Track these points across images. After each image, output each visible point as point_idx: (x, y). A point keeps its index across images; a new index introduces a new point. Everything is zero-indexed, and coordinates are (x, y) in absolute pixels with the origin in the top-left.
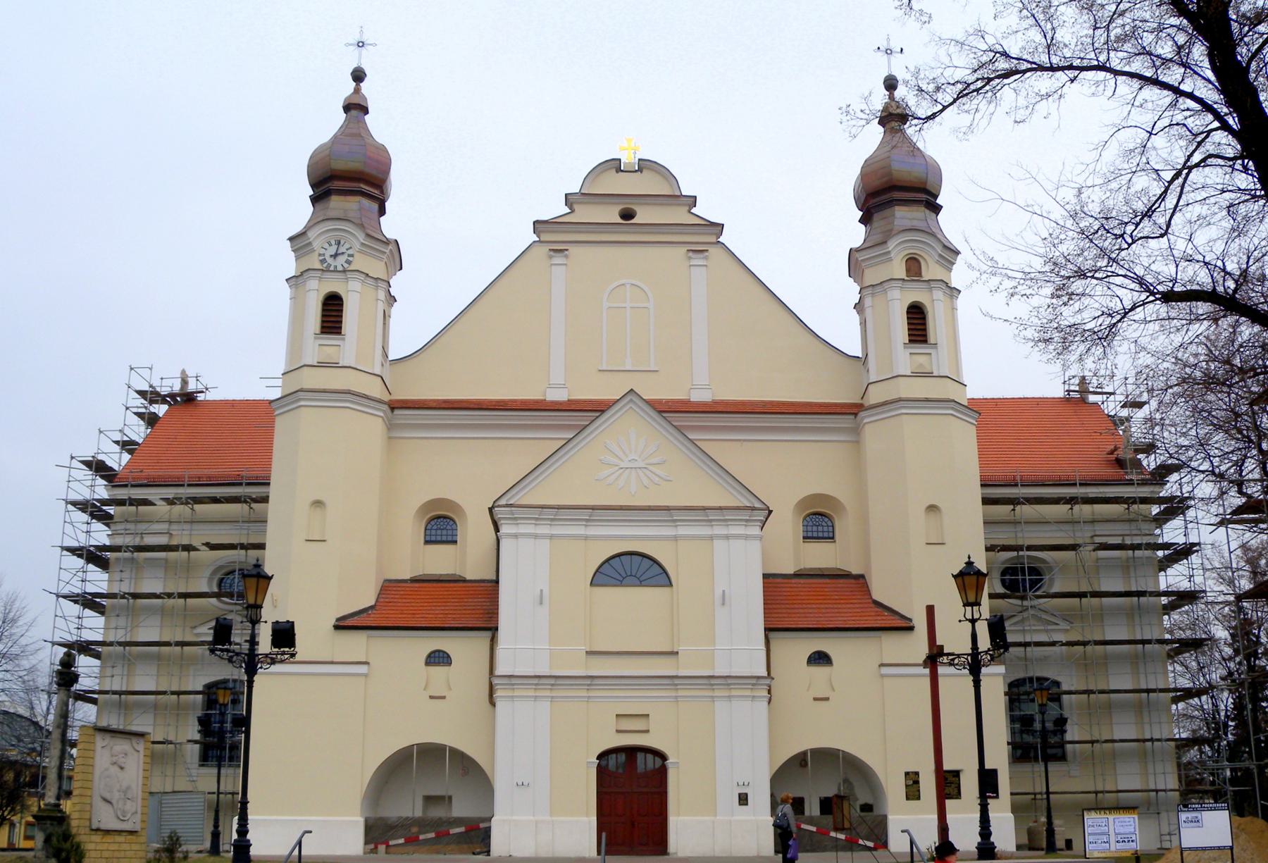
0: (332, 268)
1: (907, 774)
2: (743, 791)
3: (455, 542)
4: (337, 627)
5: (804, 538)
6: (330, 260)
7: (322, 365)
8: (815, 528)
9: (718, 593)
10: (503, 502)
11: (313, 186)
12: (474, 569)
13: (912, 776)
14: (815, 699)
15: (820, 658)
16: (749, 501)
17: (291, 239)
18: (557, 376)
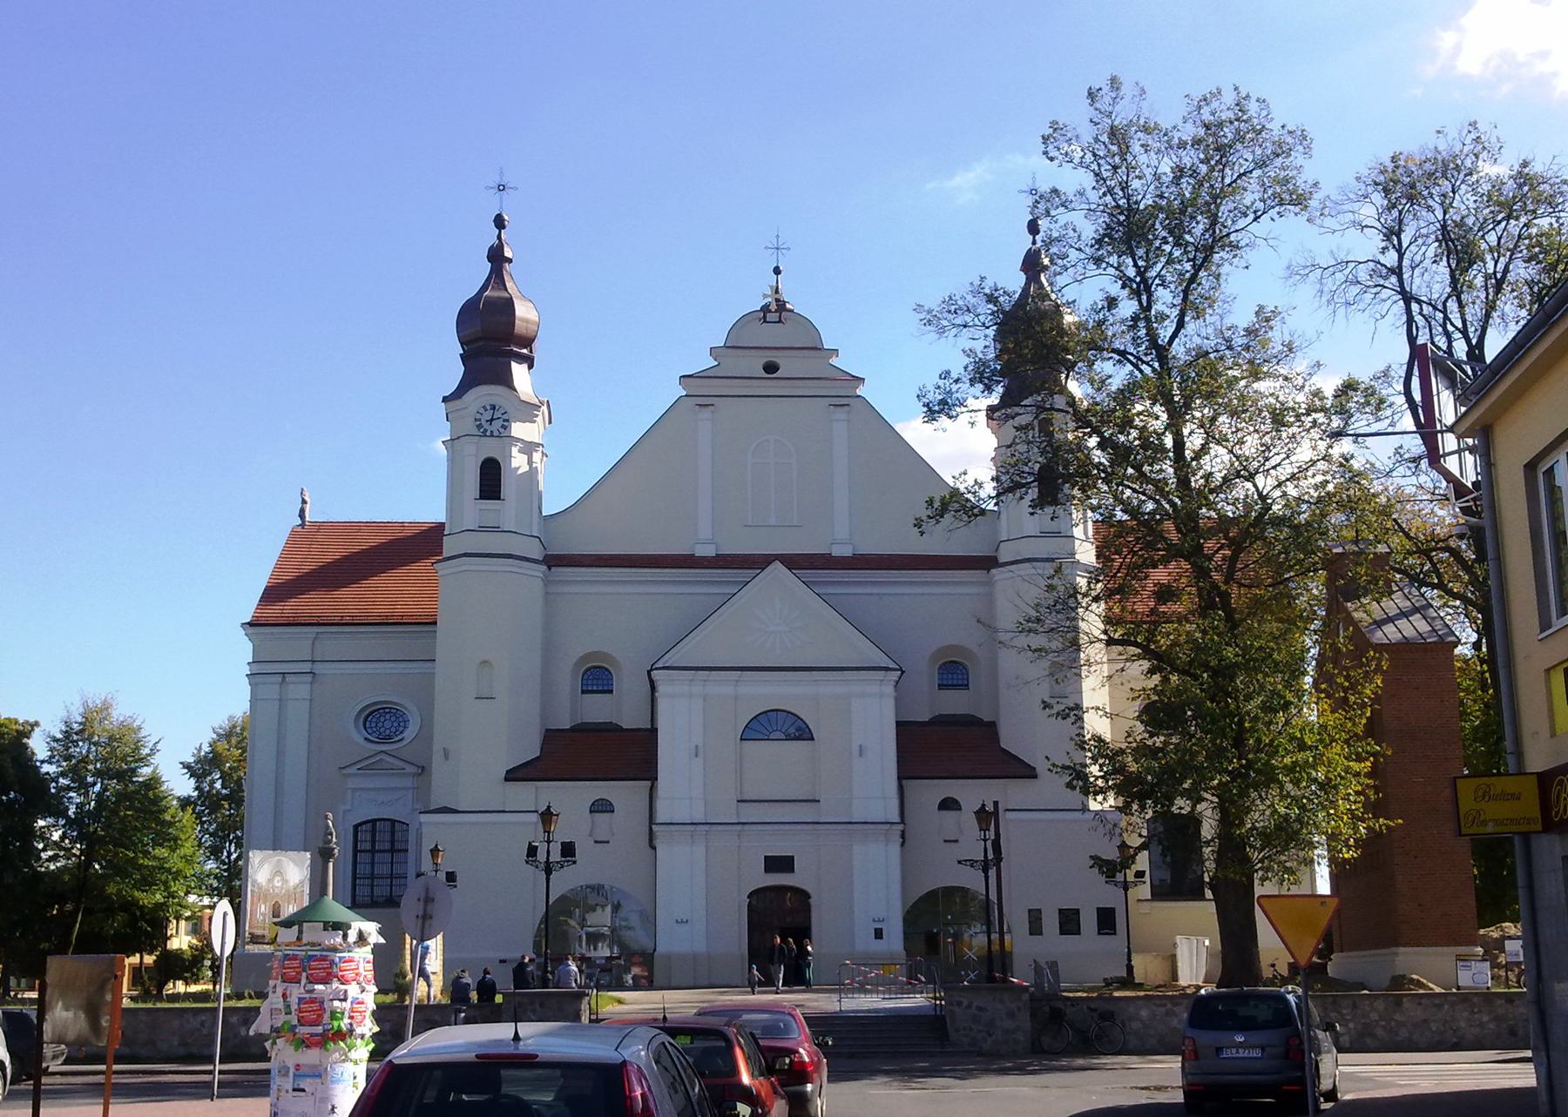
0: (488, 434)
2: (878, 926)
3: (611, 692)
4: (506, 779)
5: (939, 685)
6: (486, 426)
7: (483, 529)
8: (950, 676)
9: (855, 747)
10: (656, 666)
12: (630, 717)
14: (945, 841)
15: (949, 804)
18: (705, 532)
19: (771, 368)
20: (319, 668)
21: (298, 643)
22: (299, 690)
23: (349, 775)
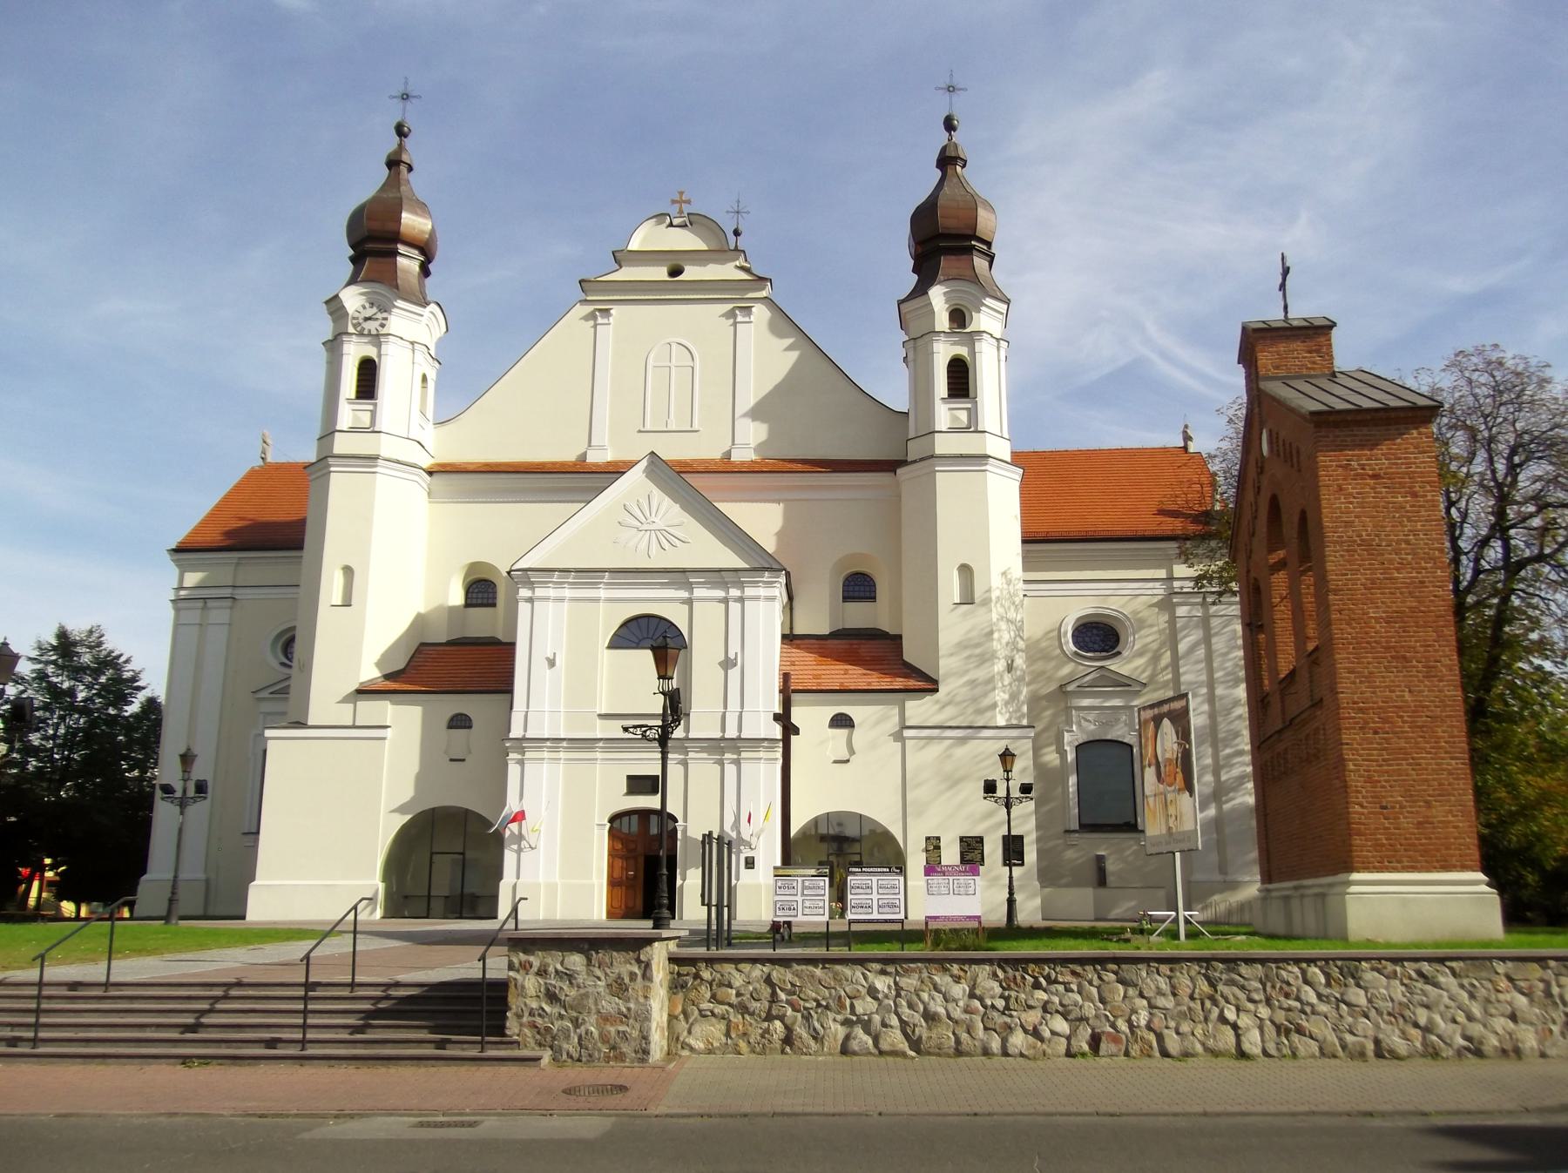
1: (928, 839)
11: (352, 247)
13: (935, 842)
16: (767, 562)
17: (327, 302)
19: (675, 272)
20: (239, 593)
21: (226, 567)
22: (219, 615)
23: (264, 699)
